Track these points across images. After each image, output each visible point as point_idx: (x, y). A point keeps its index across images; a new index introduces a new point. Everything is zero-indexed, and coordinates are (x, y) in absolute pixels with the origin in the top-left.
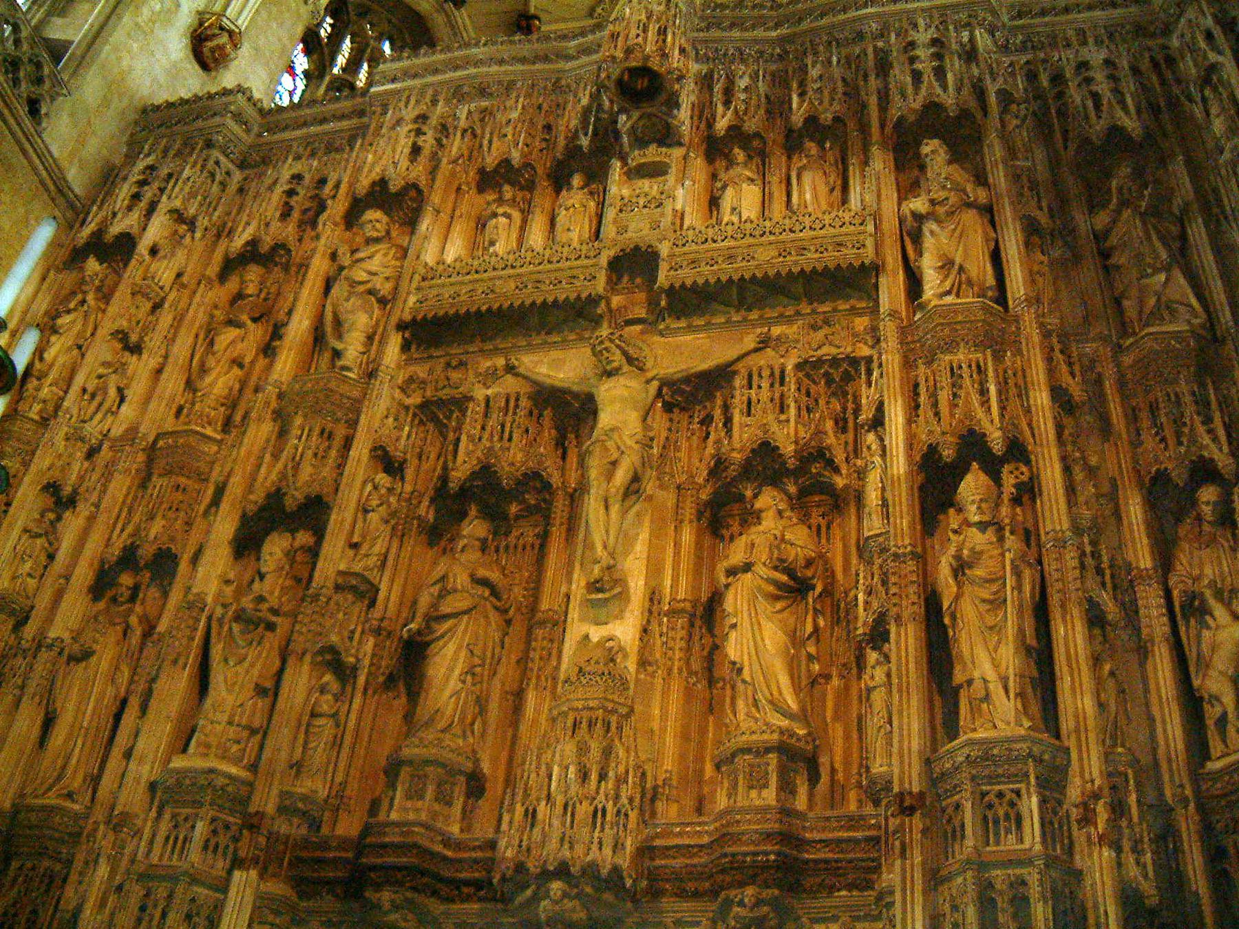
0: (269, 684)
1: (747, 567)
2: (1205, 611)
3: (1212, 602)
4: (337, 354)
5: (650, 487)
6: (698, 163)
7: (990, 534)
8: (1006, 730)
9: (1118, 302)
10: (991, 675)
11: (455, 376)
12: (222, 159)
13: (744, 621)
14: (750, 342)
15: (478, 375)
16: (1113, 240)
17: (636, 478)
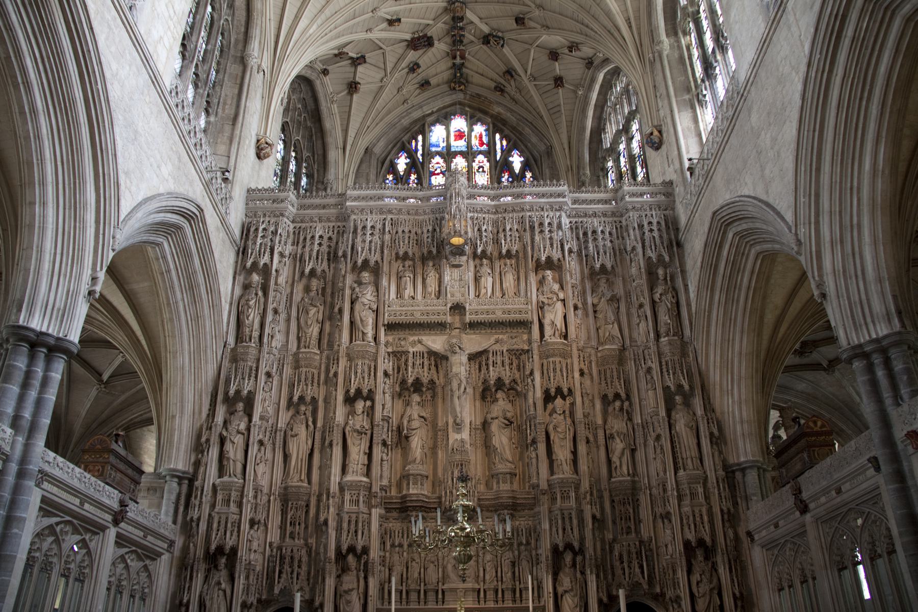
0: (367, 451)
1: (497, 418)
2: (613, 438)
3: (616, 436)
4: (363, 333)
5: (468, 390)
6: (471, 263)
7: (562, 417)
8: (567, 475)
9: (597, 330)
10: (563, 459)
11: (403, 343)
12: (287, 221)
13: (497, 433)
14: (493, 339)
15: (410, 343)
16: (598, 308)
17: (465, 389)
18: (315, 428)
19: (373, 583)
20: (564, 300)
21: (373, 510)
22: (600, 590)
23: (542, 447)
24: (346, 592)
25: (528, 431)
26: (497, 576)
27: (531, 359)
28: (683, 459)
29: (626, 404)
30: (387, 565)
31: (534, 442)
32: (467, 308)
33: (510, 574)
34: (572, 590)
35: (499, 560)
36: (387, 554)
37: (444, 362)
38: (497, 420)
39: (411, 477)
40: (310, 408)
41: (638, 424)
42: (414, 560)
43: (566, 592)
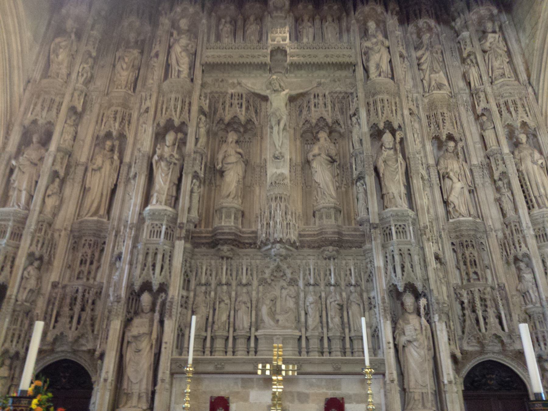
0: (176, 182)
1: (319, 155)
4: (179, 71)
7: (392, 152)
9: (422, 81)
16: (422, 61)
18: (121, 162)
19: (170, 326)
20: (388, 48)
21: (177, 243)
22: (451, 342)
23: (370, 180)
24: (135, 337)
25: (354, 166)
26: (321, 322)
27: (355, 99)
28: (535, 197)
29: (460, 145)
30: (190, 306)
31: (360, 178)
32: (288, 52)
33: (337, 320)
34: (416, 340)
35: (324, 303)
36: (192, 294)
37: (263, 103)
38: (319, 158)
39: (224, 211)
40: (117, 143)
41: (474, 165)
42: (223, 301)
43: (409, 342)
